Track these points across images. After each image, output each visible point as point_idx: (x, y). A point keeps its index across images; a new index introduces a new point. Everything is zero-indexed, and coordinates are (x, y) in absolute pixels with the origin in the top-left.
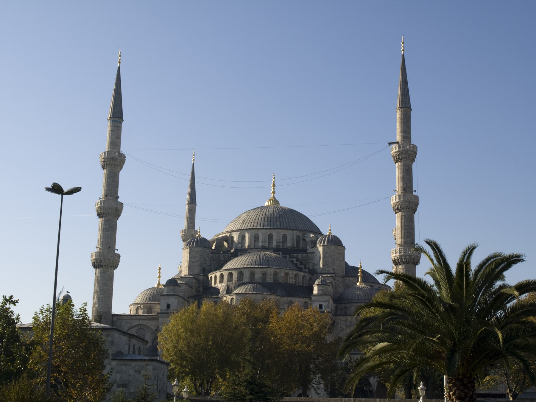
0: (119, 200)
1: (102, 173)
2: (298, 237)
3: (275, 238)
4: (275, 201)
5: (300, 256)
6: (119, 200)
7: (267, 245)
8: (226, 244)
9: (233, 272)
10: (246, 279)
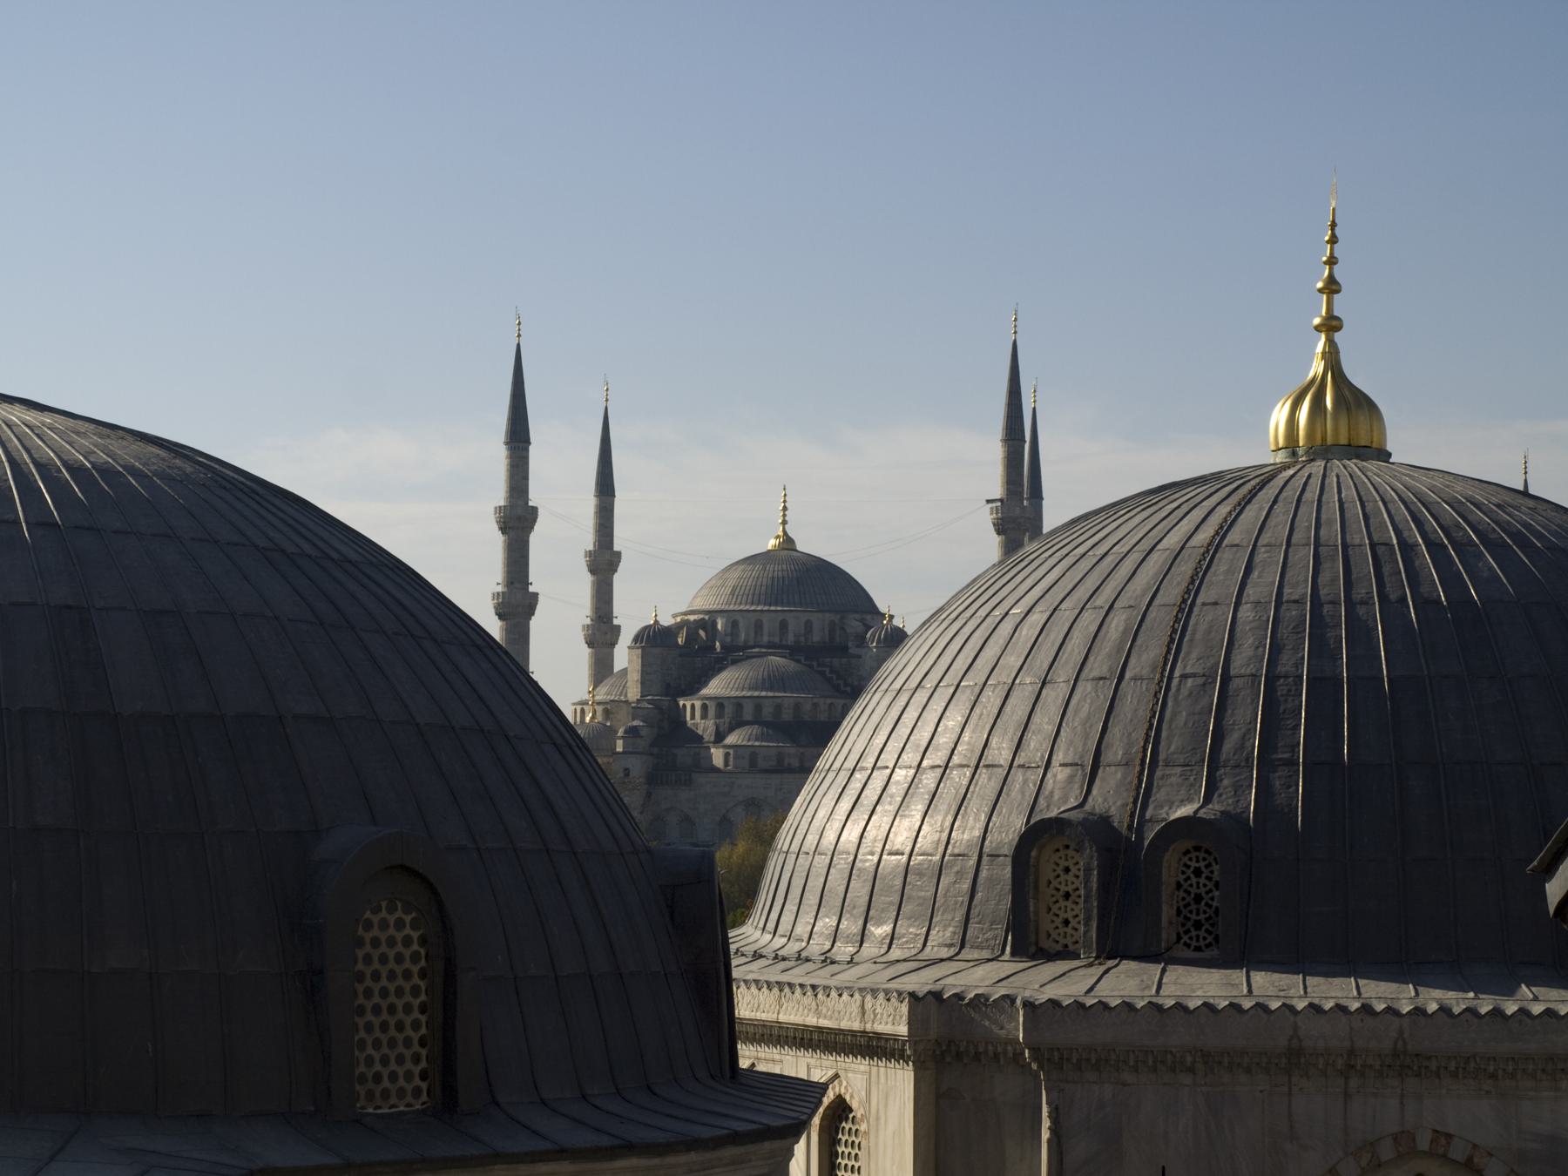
0: (531, 589)
1: (498, 540)
2: (832, 623)
3: (791, 627)
4: (788, 542)
5: (836, 662)
6: (531, 589)
7: (777, 640)
8: (702, 633)
9: (726, 703)
10: (748, 714)
